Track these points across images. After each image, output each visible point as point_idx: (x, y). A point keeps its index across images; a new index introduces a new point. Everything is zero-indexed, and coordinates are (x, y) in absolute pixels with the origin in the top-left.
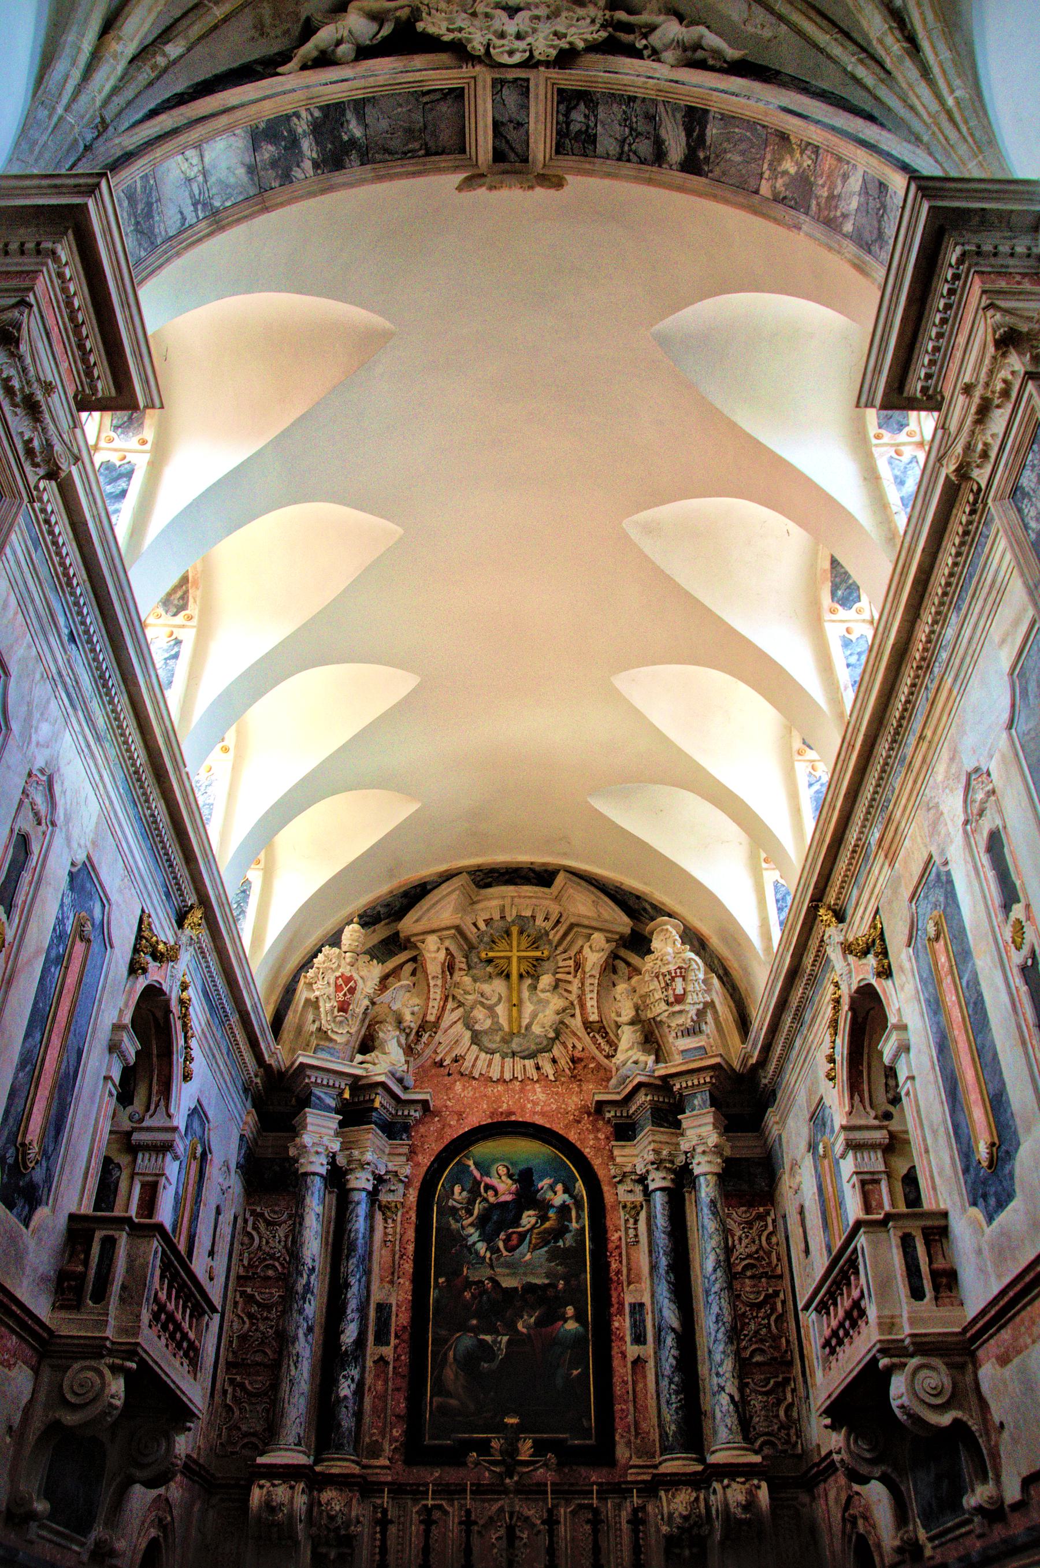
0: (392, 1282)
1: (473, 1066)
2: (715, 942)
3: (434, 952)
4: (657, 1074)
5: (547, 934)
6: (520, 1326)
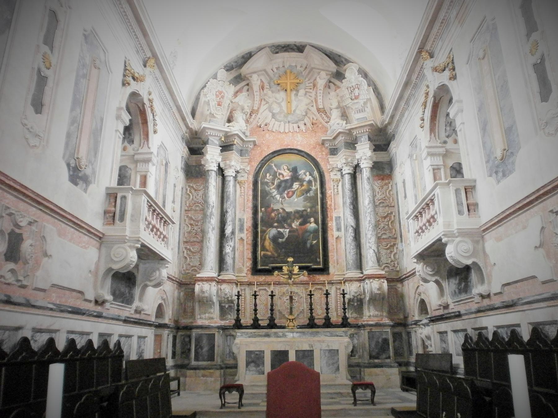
0: (244, 210)
1: (273, 127)
2: (371, 74)
3: (256, 81)
4: (346, 128)
5: (302, 73)
6: (293, 226)
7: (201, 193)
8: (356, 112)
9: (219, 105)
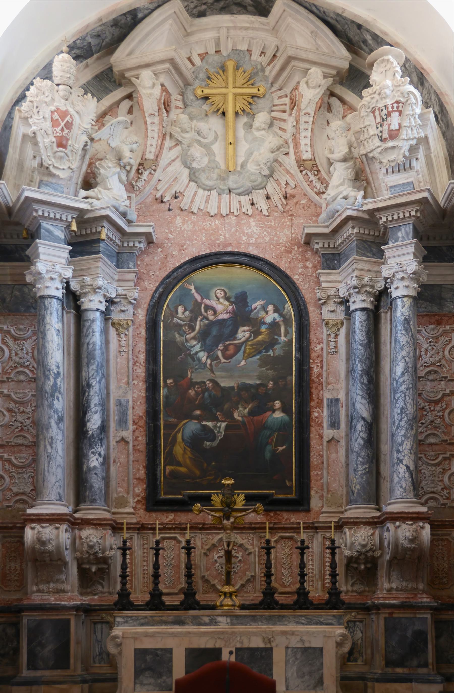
1: (192, 202)
4: (365, 208)
5: (263, 70)
6: (236, 415)
7: (28, 345)
8: (390, 170)
9: (60, 145)
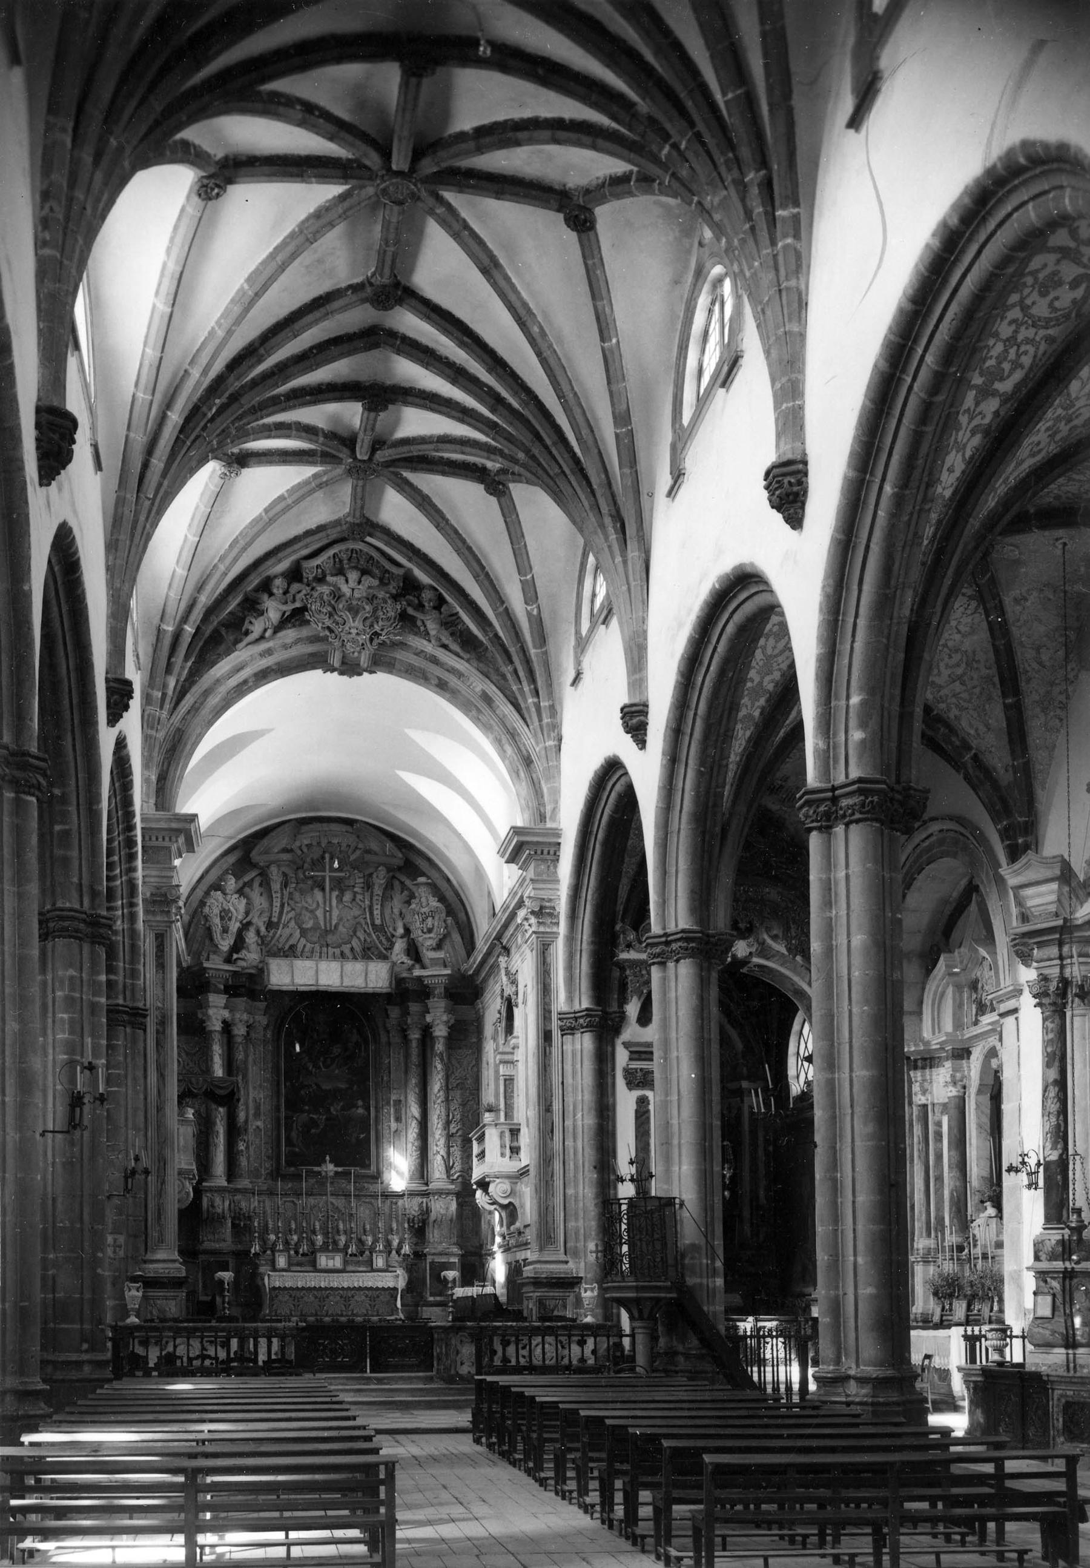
6: (332, 1109)
